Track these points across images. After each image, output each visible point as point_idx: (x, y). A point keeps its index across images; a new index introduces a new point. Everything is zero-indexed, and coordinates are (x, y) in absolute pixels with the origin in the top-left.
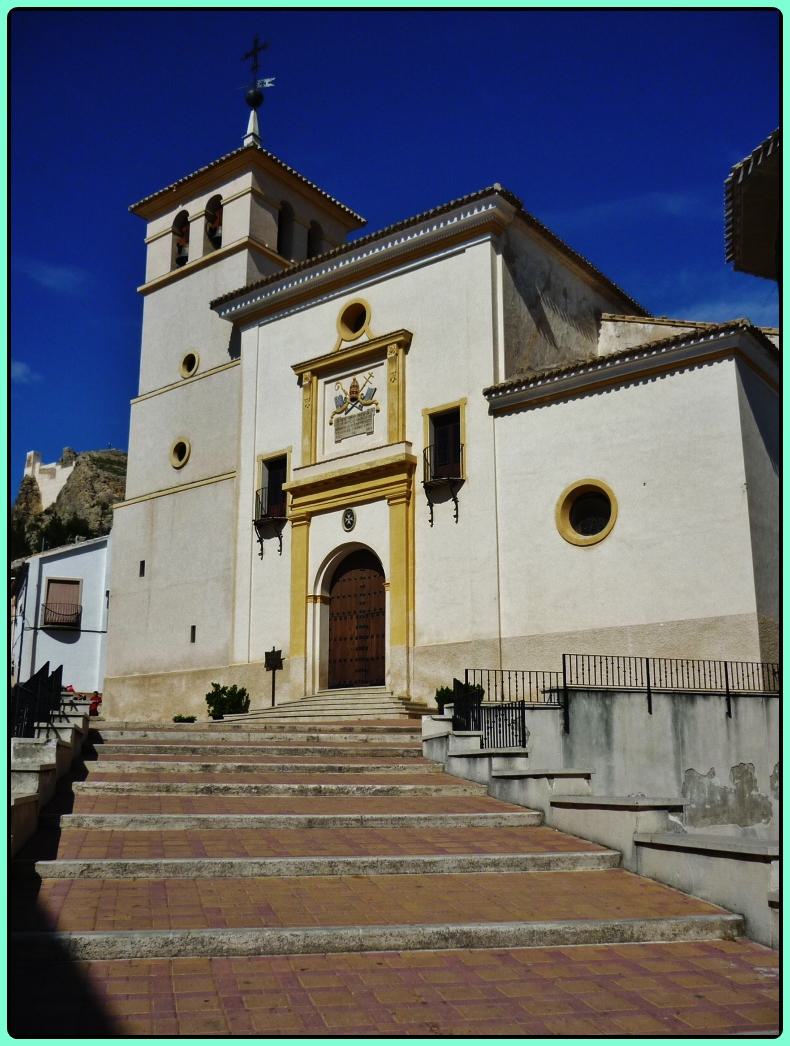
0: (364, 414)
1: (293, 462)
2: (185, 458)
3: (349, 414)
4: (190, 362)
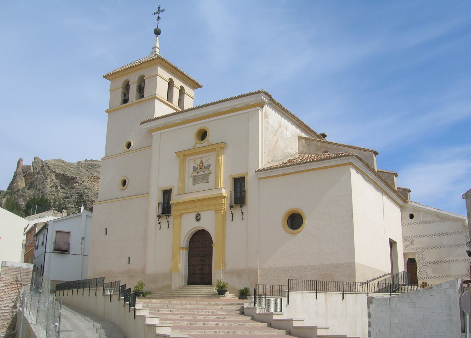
0: (205, 174)
1: (174, 193)
2: (126, 185)
3: (199, 174)
4: (129, 145)
